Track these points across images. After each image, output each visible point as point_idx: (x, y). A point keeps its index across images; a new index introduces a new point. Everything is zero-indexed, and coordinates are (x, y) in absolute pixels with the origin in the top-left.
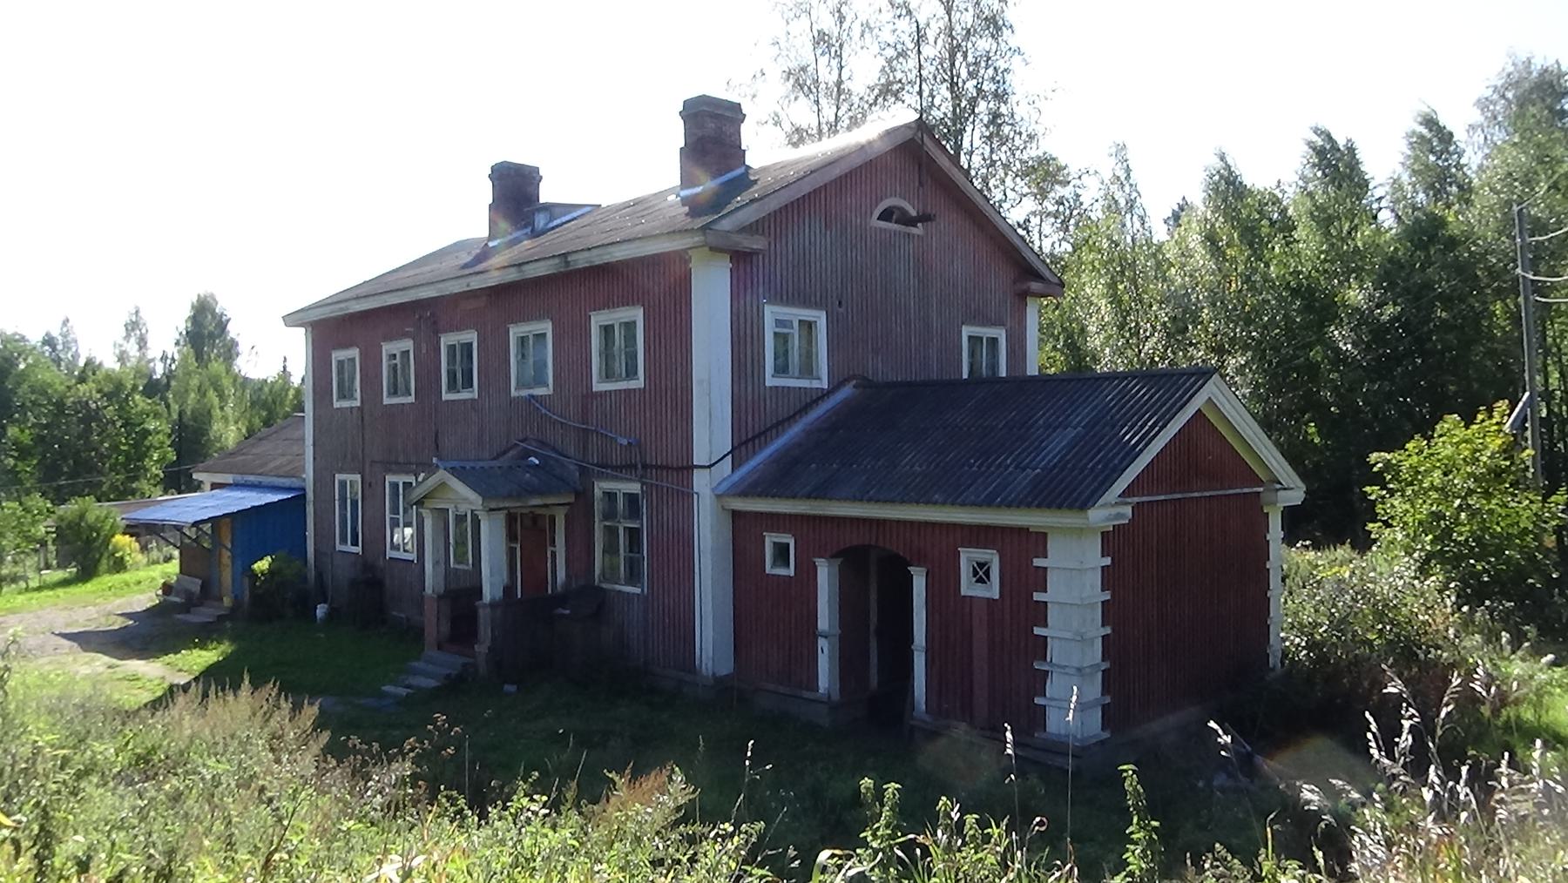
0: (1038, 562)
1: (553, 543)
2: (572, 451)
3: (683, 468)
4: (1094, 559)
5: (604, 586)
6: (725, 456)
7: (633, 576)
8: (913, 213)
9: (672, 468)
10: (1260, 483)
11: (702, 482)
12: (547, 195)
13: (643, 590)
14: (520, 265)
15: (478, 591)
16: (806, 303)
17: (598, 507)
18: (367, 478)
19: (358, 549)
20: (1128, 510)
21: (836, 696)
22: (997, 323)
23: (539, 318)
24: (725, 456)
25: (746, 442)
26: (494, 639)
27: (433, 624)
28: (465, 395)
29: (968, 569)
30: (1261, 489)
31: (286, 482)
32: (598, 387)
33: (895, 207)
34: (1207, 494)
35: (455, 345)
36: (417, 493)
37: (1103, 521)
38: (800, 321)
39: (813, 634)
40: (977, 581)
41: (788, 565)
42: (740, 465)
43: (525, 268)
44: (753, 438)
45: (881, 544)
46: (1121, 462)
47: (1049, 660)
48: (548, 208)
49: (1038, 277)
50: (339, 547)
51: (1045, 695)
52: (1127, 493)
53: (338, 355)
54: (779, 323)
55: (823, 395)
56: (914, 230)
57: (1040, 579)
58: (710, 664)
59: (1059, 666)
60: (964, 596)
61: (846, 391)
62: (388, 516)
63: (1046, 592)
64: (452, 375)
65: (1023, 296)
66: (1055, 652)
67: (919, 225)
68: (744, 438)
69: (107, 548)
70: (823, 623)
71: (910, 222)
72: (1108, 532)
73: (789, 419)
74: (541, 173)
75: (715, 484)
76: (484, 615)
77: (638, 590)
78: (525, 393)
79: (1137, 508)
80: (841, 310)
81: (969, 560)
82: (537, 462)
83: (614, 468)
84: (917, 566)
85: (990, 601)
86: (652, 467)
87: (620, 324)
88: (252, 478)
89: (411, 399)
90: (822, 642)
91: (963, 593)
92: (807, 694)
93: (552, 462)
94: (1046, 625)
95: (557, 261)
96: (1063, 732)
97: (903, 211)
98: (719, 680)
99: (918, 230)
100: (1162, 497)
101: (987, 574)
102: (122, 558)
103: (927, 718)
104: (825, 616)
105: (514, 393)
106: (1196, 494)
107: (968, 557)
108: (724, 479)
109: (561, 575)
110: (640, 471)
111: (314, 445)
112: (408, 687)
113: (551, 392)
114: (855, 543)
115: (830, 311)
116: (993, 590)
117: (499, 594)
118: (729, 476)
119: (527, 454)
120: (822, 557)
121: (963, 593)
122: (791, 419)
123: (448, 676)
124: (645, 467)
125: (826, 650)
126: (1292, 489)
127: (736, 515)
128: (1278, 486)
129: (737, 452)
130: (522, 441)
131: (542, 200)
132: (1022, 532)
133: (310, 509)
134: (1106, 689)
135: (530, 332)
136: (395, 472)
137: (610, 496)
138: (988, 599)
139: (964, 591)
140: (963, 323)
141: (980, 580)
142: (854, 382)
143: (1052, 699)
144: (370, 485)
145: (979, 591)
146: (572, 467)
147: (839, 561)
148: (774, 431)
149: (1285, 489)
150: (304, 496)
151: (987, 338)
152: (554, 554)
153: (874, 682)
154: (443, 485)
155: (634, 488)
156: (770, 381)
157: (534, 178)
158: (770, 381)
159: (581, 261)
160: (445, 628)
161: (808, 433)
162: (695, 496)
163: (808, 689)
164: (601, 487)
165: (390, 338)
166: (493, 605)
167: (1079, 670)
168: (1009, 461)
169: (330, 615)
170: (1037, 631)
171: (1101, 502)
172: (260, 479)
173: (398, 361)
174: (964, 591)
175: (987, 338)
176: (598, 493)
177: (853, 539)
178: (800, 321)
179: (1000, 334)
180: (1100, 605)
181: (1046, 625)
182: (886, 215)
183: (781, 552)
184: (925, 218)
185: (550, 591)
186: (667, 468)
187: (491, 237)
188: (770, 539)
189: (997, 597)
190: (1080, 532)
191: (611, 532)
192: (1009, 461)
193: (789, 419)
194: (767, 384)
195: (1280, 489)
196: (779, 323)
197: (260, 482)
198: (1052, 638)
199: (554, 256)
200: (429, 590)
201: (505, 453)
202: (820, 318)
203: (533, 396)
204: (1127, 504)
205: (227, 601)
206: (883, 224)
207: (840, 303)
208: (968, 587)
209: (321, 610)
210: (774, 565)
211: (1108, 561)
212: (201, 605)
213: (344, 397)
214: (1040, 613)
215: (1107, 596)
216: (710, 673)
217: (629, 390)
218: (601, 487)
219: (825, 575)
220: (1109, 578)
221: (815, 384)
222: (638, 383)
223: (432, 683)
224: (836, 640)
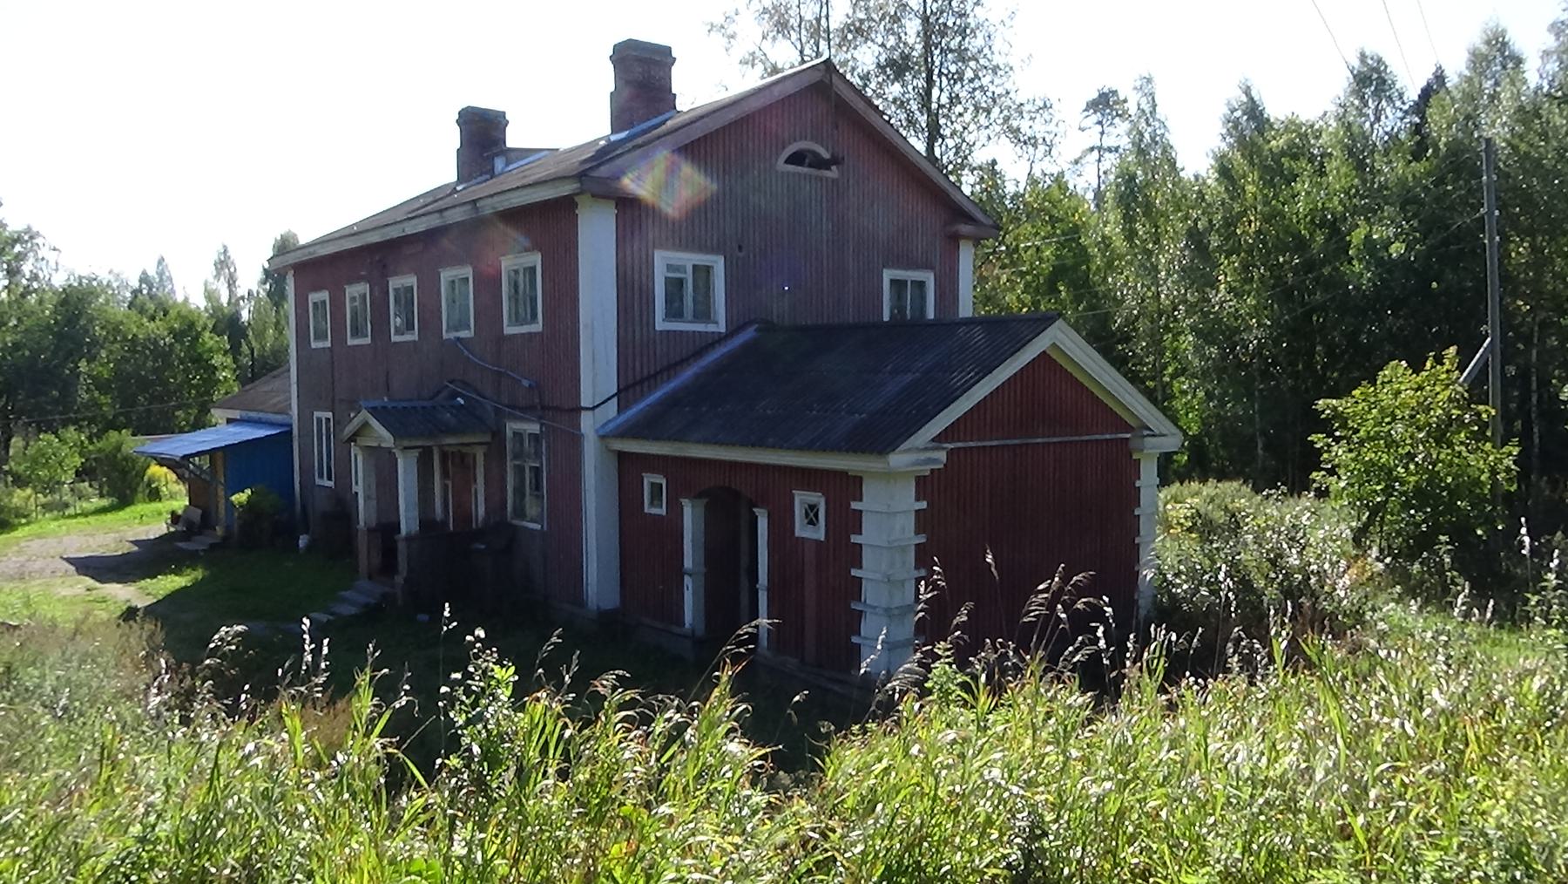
0: (855, 505)
3: (572, 410)
4: (907, 502)
5: (516, 522)
6: (609, 399)
8: (826, 155)
10: (1129, 428)
11: (588, 424)
12: (514, 139)
13: (542, 527)
16: (703, 248)
18: (336, 418)
19: (331, 484)
21: (701, 630)
22: (926, 266)
24: (609, 399)
25: (634, 385)
29: (801, 511)
30: (1128, 436)
31: (279, 418)
32: (509, 330)
33: (809, 151)
35: (399, 289)
37: (907, 466)
38: (695, 267)
39: (680, 572)
43: (446, 214)
44: (641, 382)
47: (863, 599)
49: (969, 219)
51: (860, 634)
52: (940, 438)
53: (314, 297)
54: (670, 267)
55: (720, 339)
57: (855, 522)
60: (798, 538)
61: (749, 334)
63: (861, 534)
65: (954, 240)
66: (870, 593)
67: (834, 168)
69: (143, 479)
70: (688, 563)
72: (925, 477)
74: (507, 117)
75: (598, 426)
76: (401, 546)
78: (452, 335)
79: (951, 453)
80: (741, 255)
81: (802, 502)
82: (462, 402)
83: (522, 409)
84: (761, 508)
85: (817, 542)
86: (549, 408)
87: (525, 269)
88: (253, 415)
90: (687, 580)
94: (861, 568)
95: (468, 207)
97: (816, 154)
99: (833, 173)
100: (995, 443)
102: (157, 488)
103: (768, 654)
105: (445, 336)
106: (1039, 440)
107: (801, 499)
108: (610, 421)
109: (481, 510)
112: (332, 614)
115: (728, 257)
116: (819, 533)
117: (415, 527)
118: (614, 418)
119: (455, 395)
122: (684, 362)
123: (367, 605)
124: (543, 408)
126: (1164, 435)
127: (621, 456)
129: (622, 395)
131: (510, 145)
132: (842, 475)
135: (456, 276)
137: (518, 435)
139: (798, 533)
140: (884, 267)
141: (811, 523)
142: (757, 326)
143: (865, 638)
146: (489, 408)
147: (705, 501)
148: (665, 374)
149: (1154, 436)
150: (290, 432)
151: (912, 282)
154: (366, 424)
155: (534, 428)
156: (661, 324)
157: (500, 122)
158: (661, 324)
161: (697, 376)
164: (512, 427)
165: (351, 282)
166: (409, 538)
167: (887, 610)
169: (309, 547)
170: (854, 572)
171: (902, 447)
172: (261, 415)
175: (912, 282)
176: (509, 433)
178: (695, 267)
179: (929, 278)
180: (913, 547)
181: (861, 568)
182: (796, 159)
183: (655, 489)
184: (835, 161)
185: (474, 526)
188: (649, 479)
189: (822, 539)
191: (520, 470)
194: (657, 328)
195: (1148, 435)
197: (260, 418)
198: (867, 579)
202: (718, 264)
203: (458, 339)
204: (944, 449)
205: (219, 531)
206: (791, 168)
207: (740, 248)
208: (802, 530)
209: (303, 541)
212: (200, 534)
214: (855, 555)
218: (512, 427)
219: (691, 516)
220: (923, 521)
221: (711, 328)
222: (537, 327)
223: (353, 610)
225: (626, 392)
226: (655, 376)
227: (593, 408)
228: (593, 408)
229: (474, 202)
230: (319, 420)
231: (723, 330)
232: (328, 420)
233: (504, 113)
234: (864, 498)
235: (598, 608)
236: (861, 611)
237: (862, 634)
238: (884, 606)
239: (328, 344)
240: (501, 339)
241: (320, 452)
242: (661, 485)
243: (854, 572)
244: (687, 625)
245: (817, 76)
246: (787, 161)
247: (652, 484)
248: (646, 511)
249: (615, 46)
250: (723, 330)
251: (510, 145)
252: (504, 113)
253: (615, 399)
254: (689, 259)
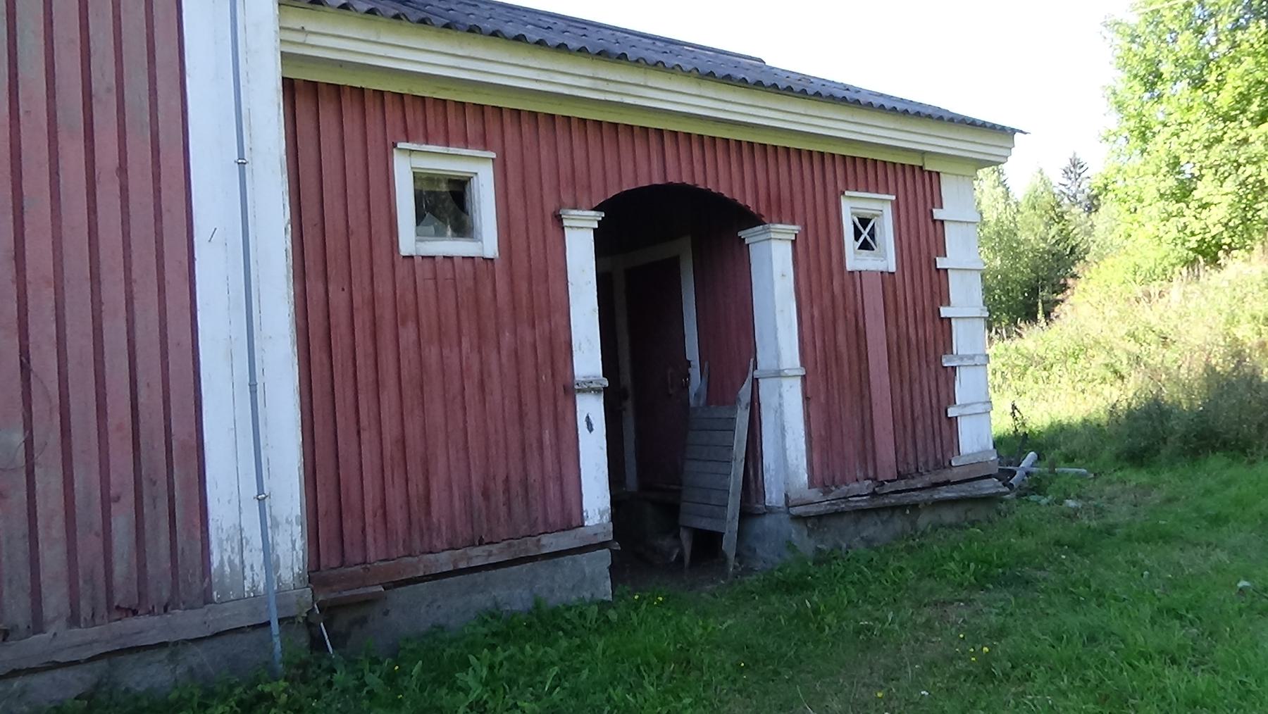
40: (860, 248)
91: (849, 268)
121: (849, 268)
138: (882, 272)
139: (851, 265)
143: (965, 405)
174: (851, 265)
189: (893, 268)
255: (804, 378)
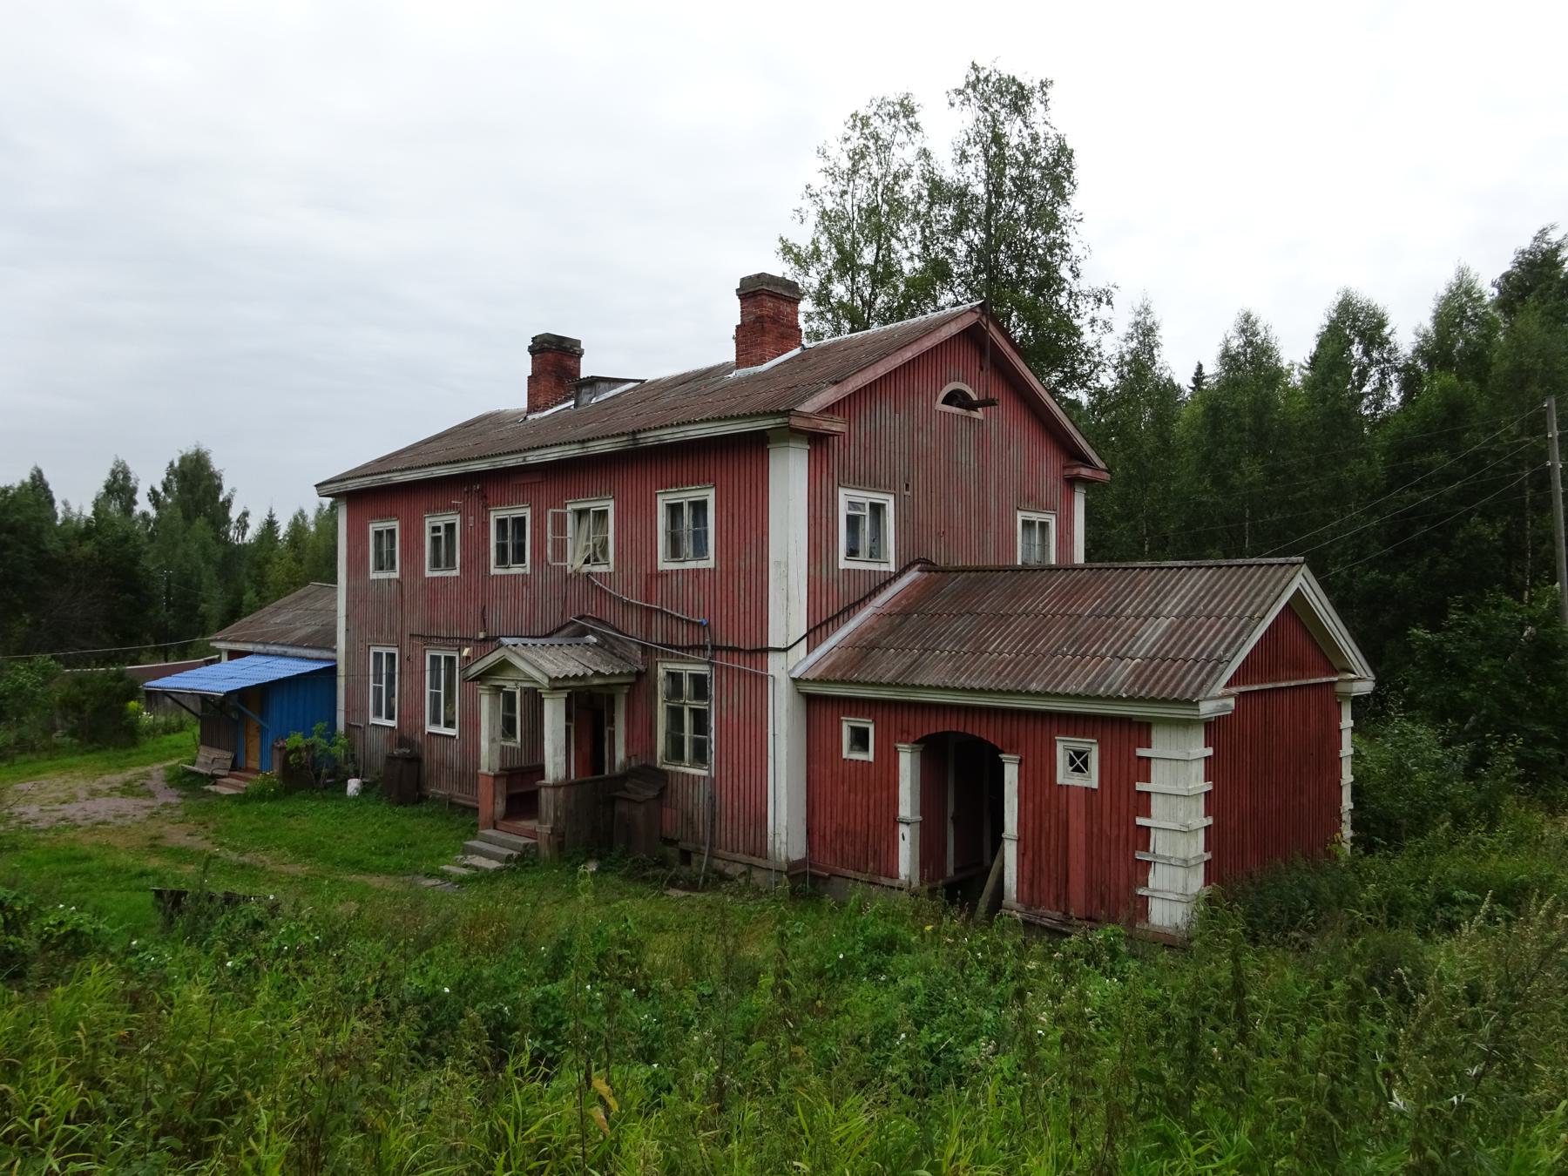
0: (1141, 752)
1: (612, 722)
2: (633, 630)
3: (756, 651)
7: (700, 756)
9: (744, 651)
11: (777, 667)
14: (583, 442)
15: (540, 771)
16: (875, 486)
17: (662, 687)
18: (406, 653)
19: (393, 723)
20: (1231, 702)
21: (916, 883)
23: (601, 496)
25: (820, 626)
26: (557, 819)
27: (490, 802)
28: (516, 570)
34: (1293, 683)
36: (475, 669)
41: (865, 748)
42: (815, 647)
44: (826, 622)
45: (969, 731)
46: (1227, 650)
47: (1152, 849)
48: (594, 382)
50: (373, 720)
52: (1228, 685)
53: (374, 527)
54: (853, 505)
56: (975, 415)
57: (1144, 768)
58: (784, 848)
59: (1164, 857)
62: (428, 690)
64: (502, 549)
66: (1159, 843)
68: (818, 622)
71: (972, 406)
73: (858, 603)
75: (790, 668)
77: (705, 773)
79: (1240, 697)
82: (595, 640)
83: (682, 648)
84: (1010, 753)
86: (721, 649)
89: (456, 573)
90: (903, 830)
92: (885, 881)
93: (611, 640)
96: (1166, 923)
98: (793, 865)
99: (979, 414)
101: (1085, 763)
104: (907, 805)
109: (620, 755)
110: (709, 653)
111: (347, 616)
112: (466, 866)
113: (612, 569)
114: (940, 730)
116: (1092, 779)
118: (805, 659)
120: (906, 742)
124: (715, 648)
125: (907, 837)
128: (1352, 676)
130: (579, 618)
131: (585, 373)
133: (341, 682)
134: (1208, 880)
136: (438, 647)
137: (675, 677)
139: (1060, 780)
141: (1077, 769)
143: (1155, 890)
144: (408, 659)
145: (1077, 781)
150: (333, 670)
152: (612, 734)
153: (950, 871)
155: (702, 669)
156: (844, 564)
158: (844, 564)
159: (650, 439)
160: (500, 807)
161: (880, 616)
162: (770, 679)
163: (886, 876)
165: (433, 510)
166: (556, 786)
167: (1186, 861)
168: (1104, 650)
169: (365, 789)
170: (1140, 821)
173: (442, 534)
174: (1060, 780)
176: (661, 673)
177: (936, 726)
184: (986, 403)
185: (607, 772)
186: (739, 650)
187: (533, 408)
189: (1095, 785)
190: (1187, 724)
191: (675, 715)
192: (1104, 650)
193: (858, 603)
194: (841, 567)
196: (853, 505)
199: (623, 434)
200: (484, 769)
201: (559, 629)
204: (1230, 696)
206: (947, 408)
208: (1064, 775)
209: (353, 785)
210: (851, 749)
211: (1210, 752)
213: (381, 568)
214: (1143, 803)
215: (1209, 786)
216: (783, 858)
217: (698, 570)
219: (907, 763)
220: (1212, 768)
221: (884, 568)
222: (709, 563)
223: (493, 865)
224: (918, 826)
225: (816, 632)
226: (837, 616)
227: (786, 650)
228: (786, 650)
229: (634, 433)
230: (378, 656)
231: (893, 570)
232: (391, 657)
233: (579, 342)
234: (1154, 744)
235: (788, 859)
236: (1149, 863)
237: (1151, 886)
238: (1182, 856)
239: (396, 575)
240: (655, 576)
241: (378, 691)
242: (866, 731)
243: (1140, 821)
244: (902, 877)
245: (970, 320)
246: (944, 402)
247: (853, 729)
248: (845, 755)
249: (743, 280)
250: (893, 570)
251: (585, 373)
252: (578, 343)
253: (805, 639)
254: (867, 497)
255: (1019, 841)
